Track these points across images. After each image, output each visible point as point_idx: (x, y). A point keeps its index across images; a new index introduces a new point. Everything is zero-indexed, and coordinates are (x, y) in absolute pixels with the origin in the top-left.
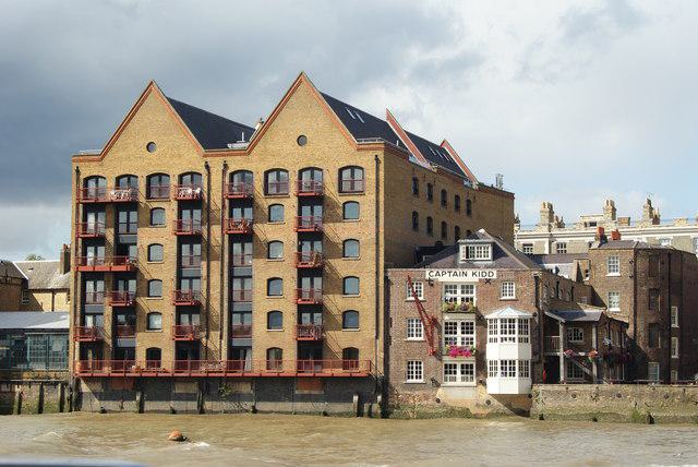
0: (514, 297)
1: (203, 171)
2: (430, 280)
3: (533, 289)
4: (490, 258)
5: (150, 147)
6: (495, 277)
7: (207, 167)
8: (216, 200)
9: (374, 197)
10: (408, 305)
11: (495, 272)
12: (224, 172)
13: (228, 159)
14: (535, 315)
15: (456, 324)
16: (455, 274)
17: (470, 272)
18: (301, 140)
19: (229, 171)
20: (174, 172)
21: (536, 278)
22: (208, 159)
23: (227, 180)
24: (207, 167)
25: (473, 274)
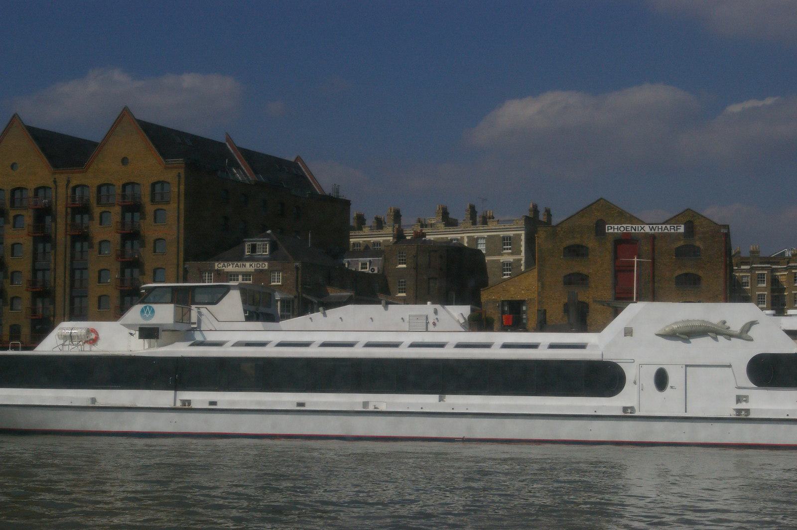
0: (280, 283)
1: (52, 185)
2: (218, 270)
5: (13, 166)
6: (266, 268)
7: (55, 182)
8: (61, 208)
9: (176, 205)
11: (266, 264)
12: (67, 185)
14: (295, 297)
16: (237, 266)
17: (248, 264)
18: (125, 161)
20: (32, 186)
21: (297, 268)
23: (70, 191)
24: (55, 182)
25: (251, 265)
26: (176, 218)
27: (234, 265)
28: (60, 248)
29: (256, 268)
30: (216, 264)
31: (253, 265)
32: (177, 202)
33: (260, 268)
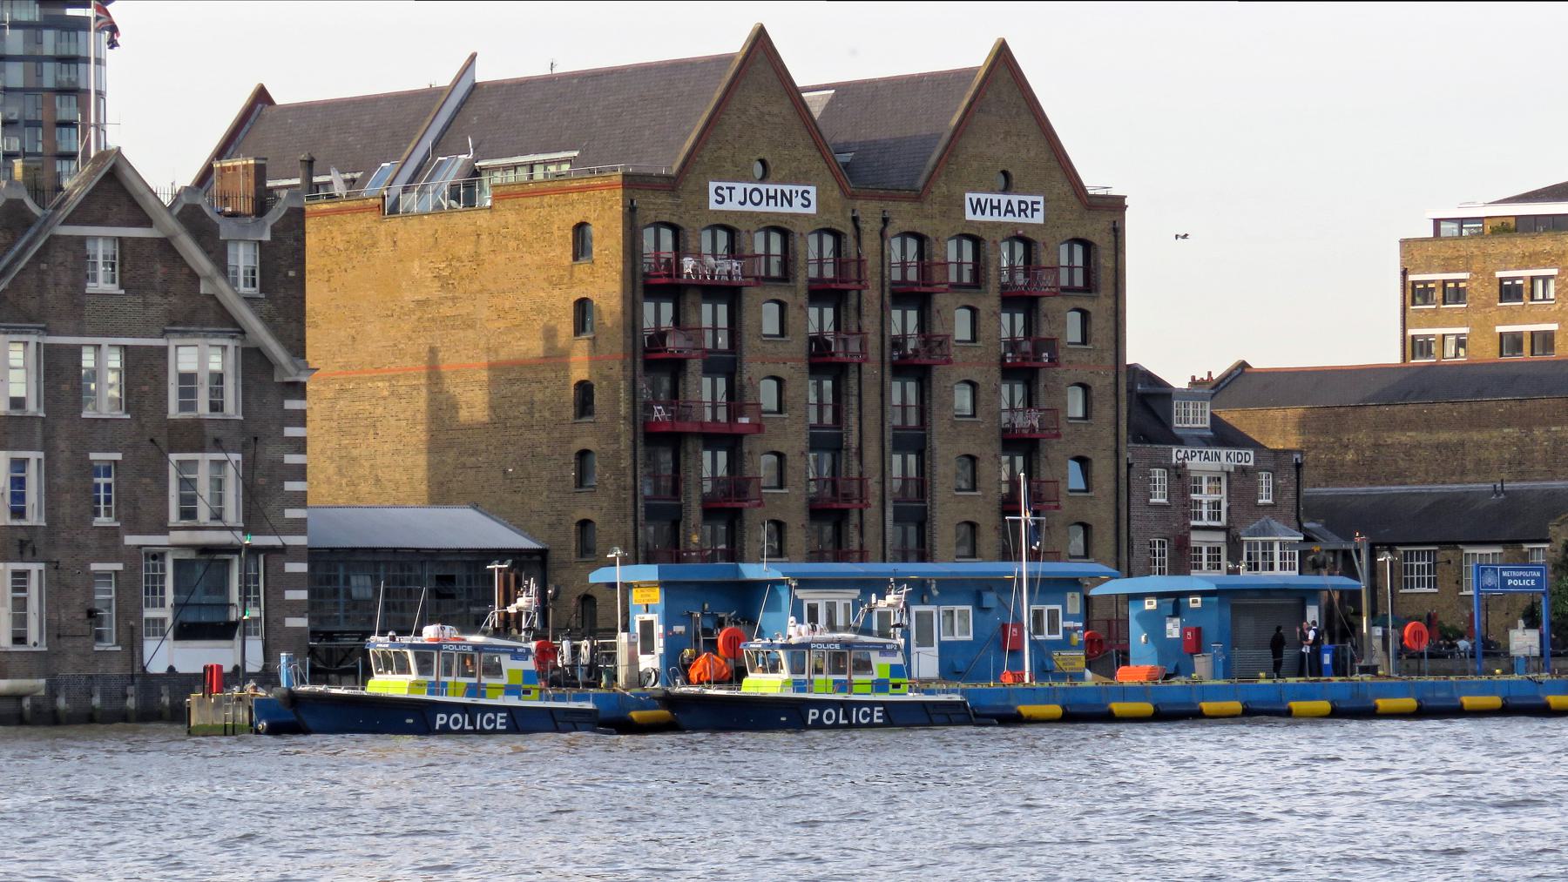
0: (1270, 501)
1: (848, 229)
3: (1293, 488)
4: (1208, 424)
7: (855, 220)
9: (1110, 302)
10: (1152, 514)
11: (1252, 453)
12: (882, 234)
13: (890, 206)
15: (1201, 551)
17: (1223, 453)
19: (890, 231)
22: (858, 204)
24: (855, 220)
25: (1228, 456)
26: (1112, 334)
27: (1203, 455)
28: (871, 399)
29: (1236, 463)
30: (1175, 451)
31: (1232, 456)
32: (1111, 292)
33: (1243, 463)
